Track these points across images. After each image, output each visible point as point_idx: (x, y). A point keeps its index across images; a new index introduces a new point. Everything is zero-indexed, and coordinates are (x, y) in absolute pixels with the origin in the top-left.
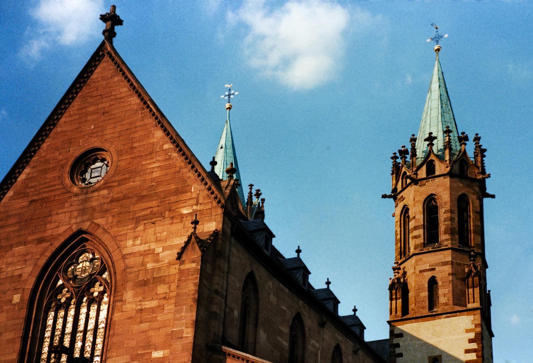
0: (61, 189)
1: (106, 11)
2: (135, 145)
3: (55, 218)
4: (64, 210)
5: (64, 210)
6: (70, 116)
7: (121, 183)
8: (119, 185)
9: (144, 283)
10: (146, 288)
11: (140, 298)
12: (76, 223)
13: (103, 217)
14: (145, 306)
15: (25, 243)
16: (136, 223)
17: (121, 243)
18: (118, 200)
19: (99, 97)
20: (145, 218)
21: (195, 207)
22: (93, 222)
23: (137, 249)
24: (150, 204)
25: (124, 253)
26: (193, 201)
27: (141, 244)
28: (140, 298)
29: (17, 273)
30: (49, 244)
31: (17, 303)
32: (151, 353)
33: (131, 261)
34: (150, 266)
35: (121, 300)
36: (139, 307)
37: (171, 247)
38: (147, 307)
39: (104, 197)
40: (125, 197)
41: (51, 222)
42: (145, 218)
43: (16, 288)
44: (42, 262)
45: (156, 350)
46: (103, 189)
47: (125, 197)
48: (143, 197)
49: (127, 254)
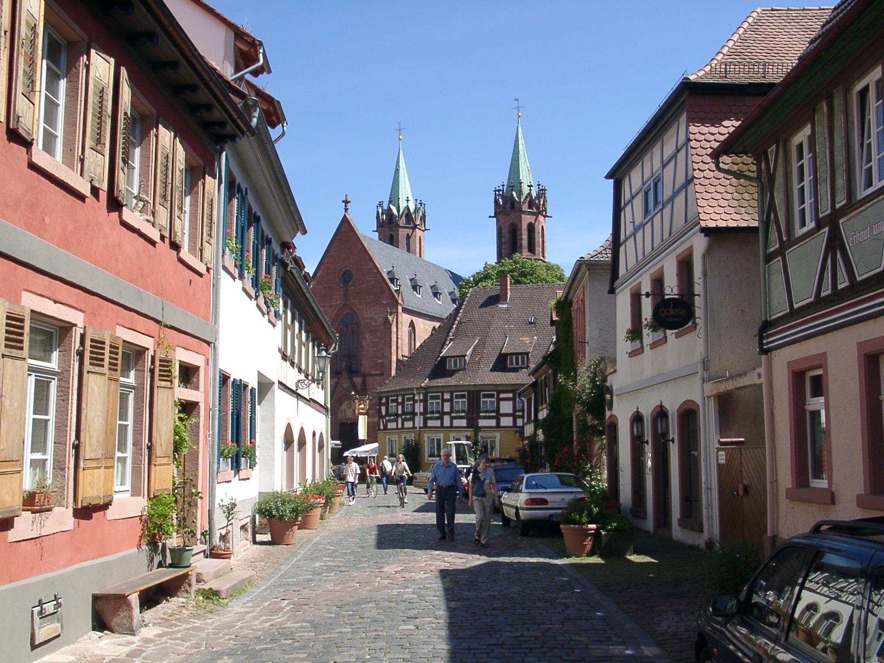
2: (363, 268)
9: (372, 331)
11: (371, 337)
23: (368, 316)
34: (374, 324)
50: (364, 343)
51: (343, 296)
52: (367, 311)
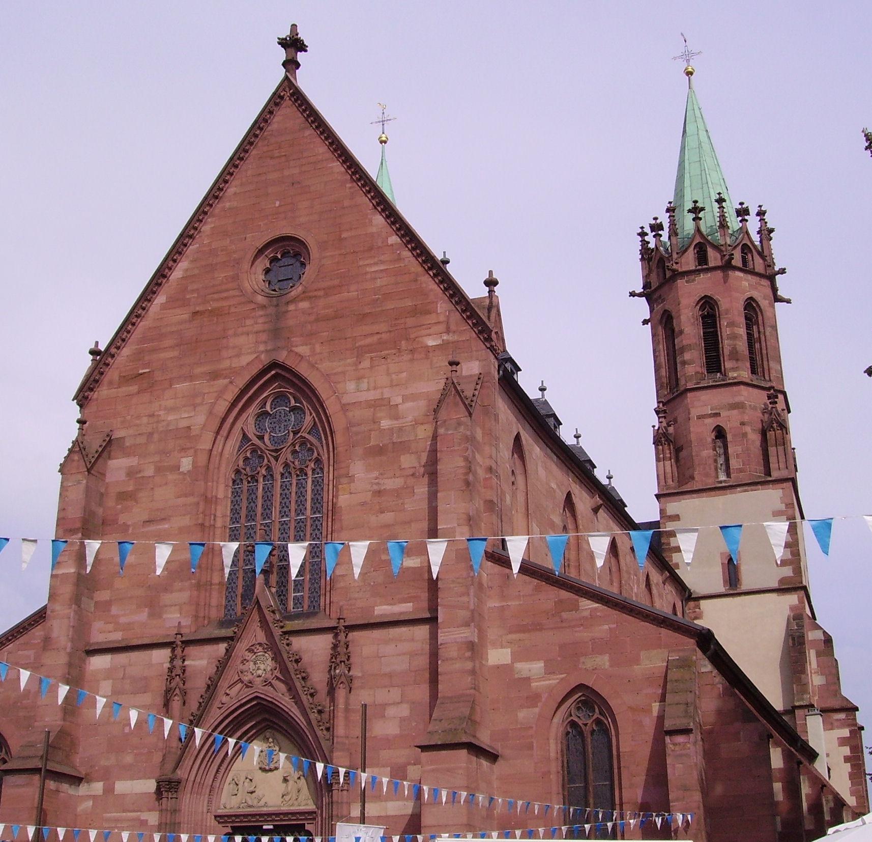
0: (237, 296)
1: (285, 33)
3: (233, 341)
4: (245, 329)
5: (245, 329)
6: (242, 185)
7: (328, 292)
8: (326, 295)
9: (380, 451)
10: (384, 458)
11: (376, 474)
12: (267, 351)
13: (306, 345)
15: (191, 378)
16: (357, 357)
17: (338, 386)
18: (327, 319)
19: (283, 159)
20: (370, 348)
22: (291, 351)
24: (376, 328)
25: (344, 401)
26: (442, 328)
27: (368, 390)
28: (376, 474)
29: (183, 424)
30: (227, 381)
31: (188, 471)
33: (357, 414)
34: (385, 424)
35: (347, 476)
36: (375, 487)
37: (413, 397)
39: (304, 312)
40: (337, 316)
41: (227, 348)
42: (370, 348)
44: (222, 407)
46: (302, 300)
47: (337, 316)
49: (349, 404)
50: (343, 500)
51: (264, 337)
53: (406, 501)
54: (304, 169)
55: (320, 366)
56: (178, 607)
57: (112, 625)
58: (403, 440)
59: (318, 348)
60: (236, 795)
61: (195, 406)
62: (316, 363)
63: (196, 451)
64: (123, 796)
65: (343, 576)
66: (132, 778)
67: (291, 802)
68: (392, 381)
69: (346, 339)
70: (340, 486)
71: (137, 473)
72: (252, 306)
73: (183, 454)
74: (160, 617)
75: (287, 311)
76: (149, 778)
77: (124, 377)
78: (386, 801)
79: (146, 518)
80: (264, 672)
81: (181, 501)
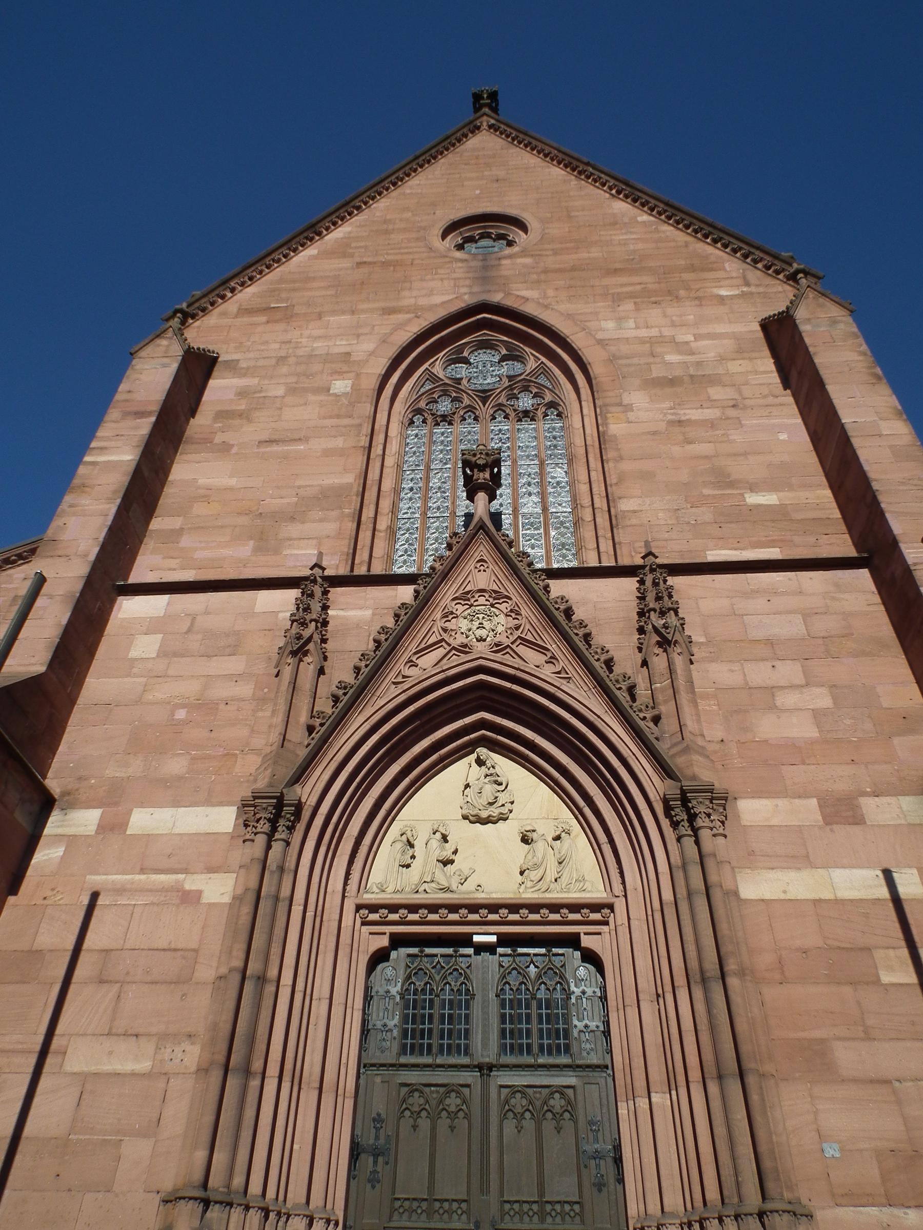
0: (423, 252)
2: (572, 214)
11: (667, 404)
14: (687, 417)
16: (613, 301)
21: (745, 289)
24: (636, 279)
25: (600, 336)
26: (740, 281)
31: (345, 393)
32: (742, 495)
36: (670, 417)
38: (693, 418)
42: (631, 296)
43: (339, 370)
45: (752, 491)
47: (574, 269)
48: (616, 270)
52: (620, 319)
53: (729, 432)
54: (510, 172)
55: (556, 307)
56: (314, 542)
57: (177, 561)
58: (707, 373)
59: (551, 293)
60: (408, 866)
61: (358, 336)
62: (550, 304)
63: (358, 375)
64: (148, 839)
65: (635, 512)
66: (176, 804)
67: (543, 885)
68: (672, 321)
69: (593, 286)
70: (609, 415)
71: (255, 392)
72: (447, 260)
73: (336, 377)
74: (277, 551)
75: (500, 265)
76: (221, 804)
77: (246, 309)
78: (826, 866)
79: (265, 437)
80: (491, 633)
81: (328, 422)
